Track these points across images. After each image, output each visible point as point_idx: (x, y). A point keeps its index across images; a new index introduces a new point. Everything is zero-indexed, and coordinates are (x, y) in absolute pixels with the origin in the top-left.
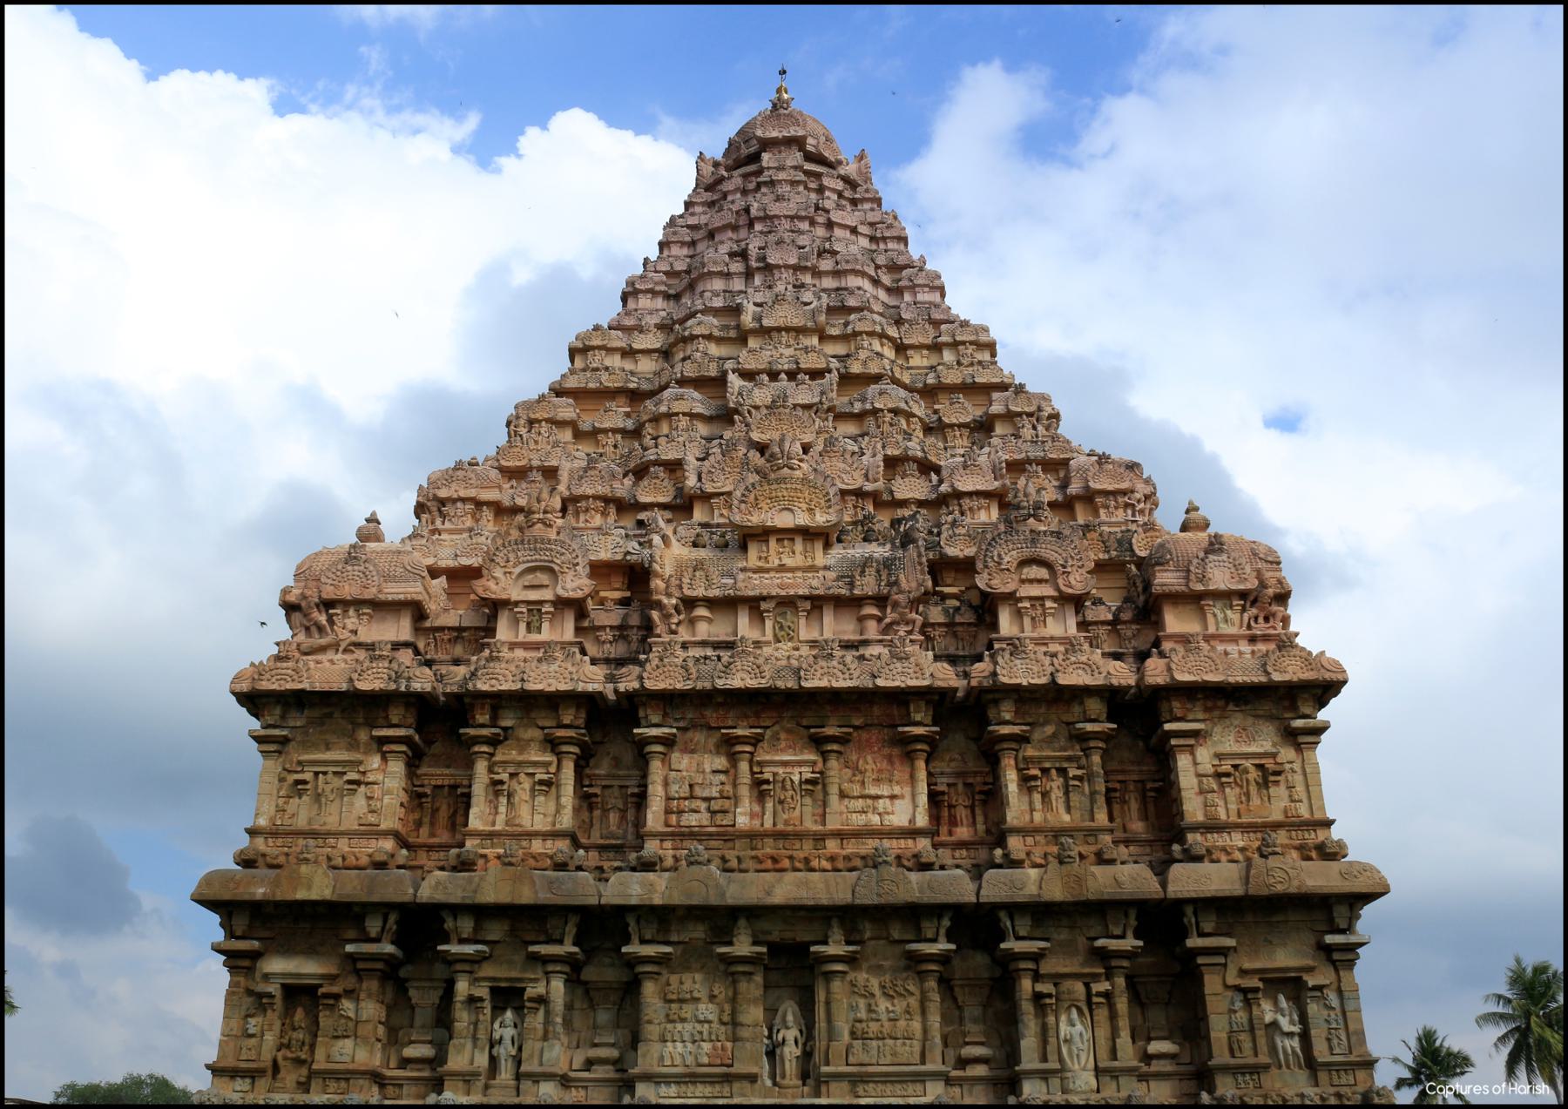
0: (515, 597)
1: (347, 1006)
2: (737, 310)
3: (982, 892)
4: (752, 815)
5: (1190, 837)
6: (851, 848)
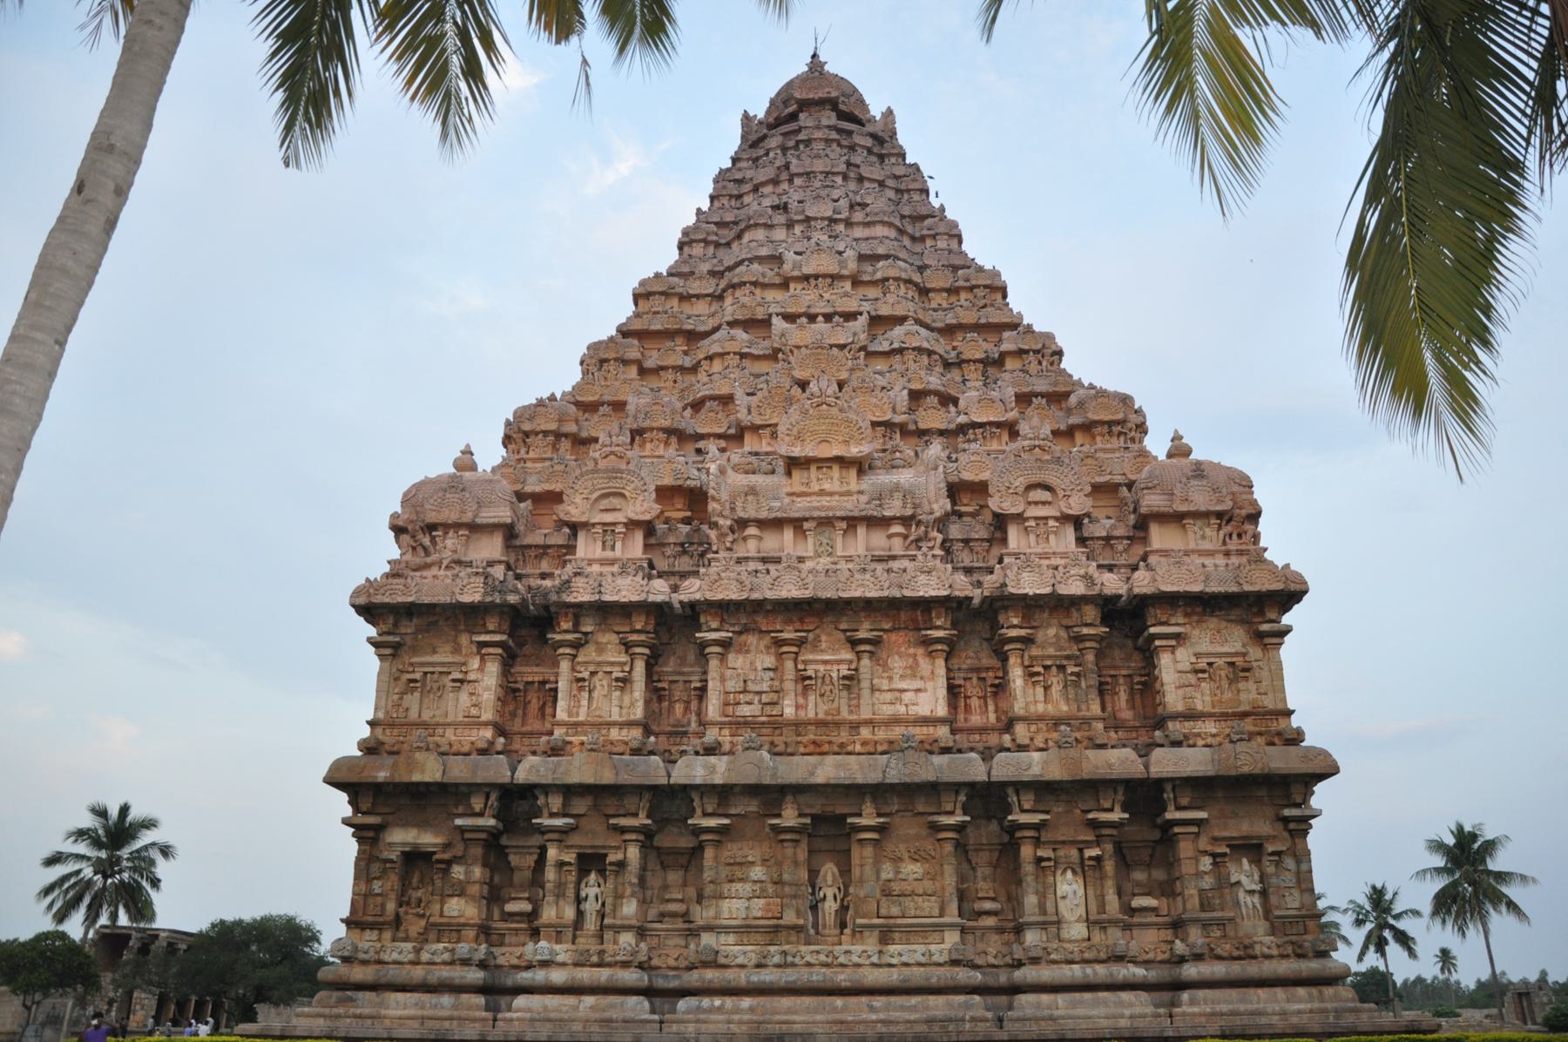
1: (458, 872)
2: (777, 259)
3: (994, 773)
4: (797, 707)
5: (1170, 725)
6: (882, 734)
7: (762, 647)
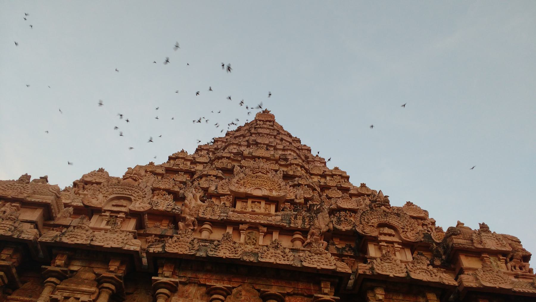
0: (106, 208)
7: (198, 295)
